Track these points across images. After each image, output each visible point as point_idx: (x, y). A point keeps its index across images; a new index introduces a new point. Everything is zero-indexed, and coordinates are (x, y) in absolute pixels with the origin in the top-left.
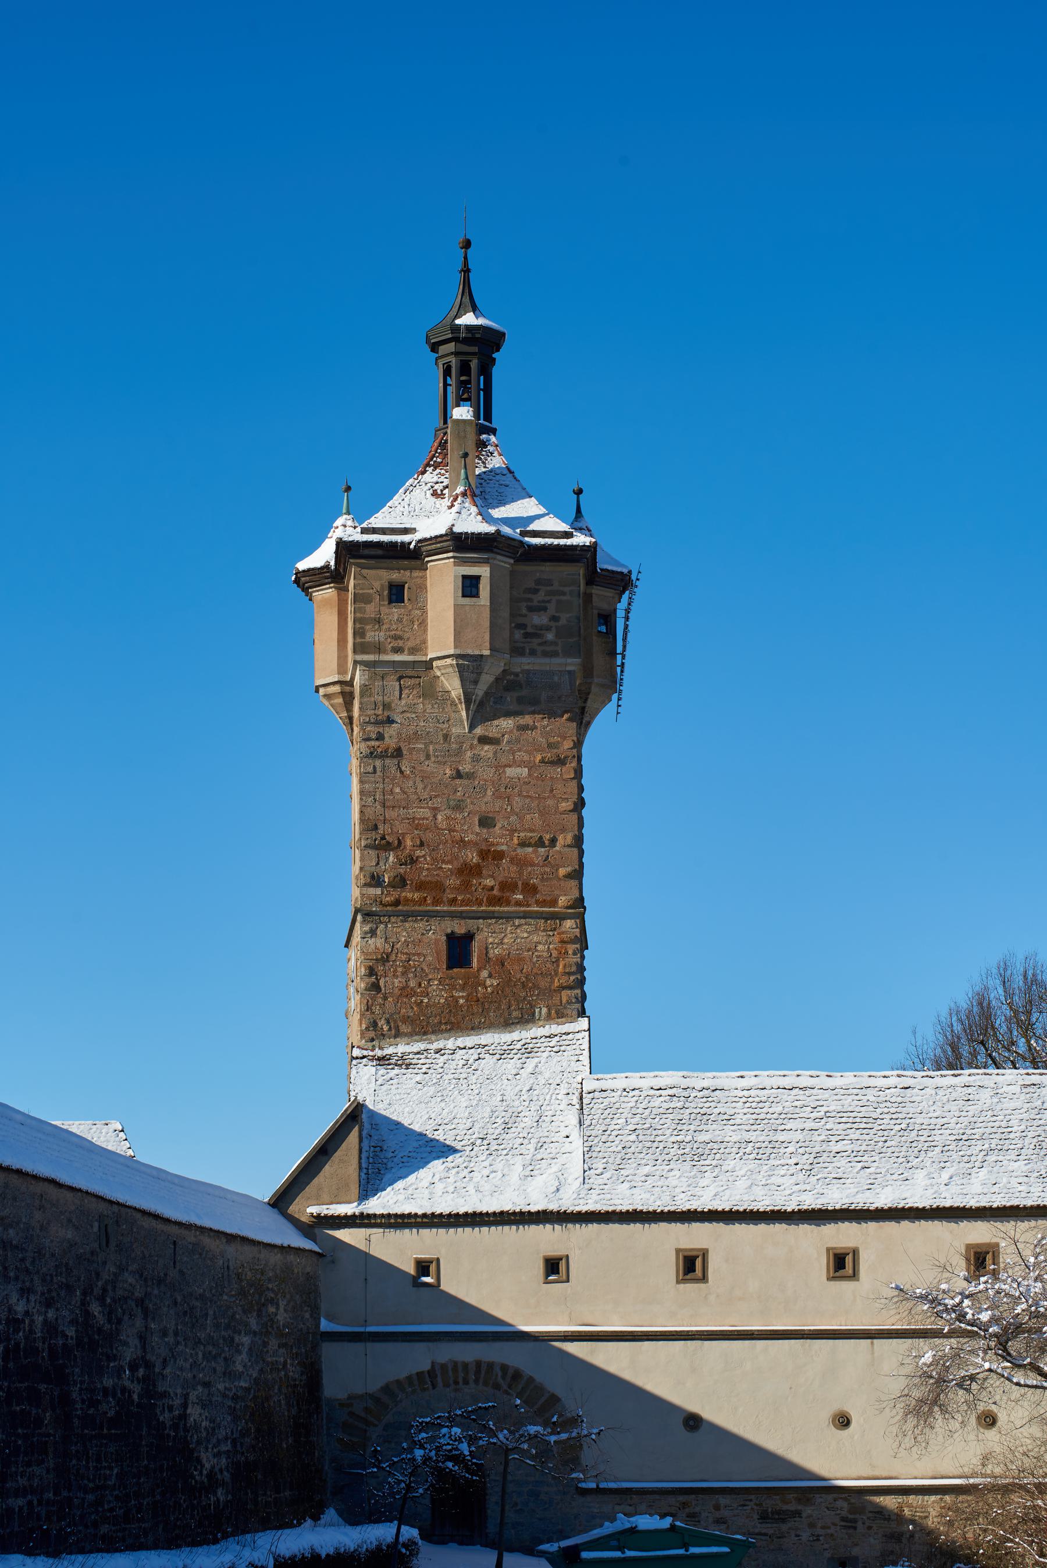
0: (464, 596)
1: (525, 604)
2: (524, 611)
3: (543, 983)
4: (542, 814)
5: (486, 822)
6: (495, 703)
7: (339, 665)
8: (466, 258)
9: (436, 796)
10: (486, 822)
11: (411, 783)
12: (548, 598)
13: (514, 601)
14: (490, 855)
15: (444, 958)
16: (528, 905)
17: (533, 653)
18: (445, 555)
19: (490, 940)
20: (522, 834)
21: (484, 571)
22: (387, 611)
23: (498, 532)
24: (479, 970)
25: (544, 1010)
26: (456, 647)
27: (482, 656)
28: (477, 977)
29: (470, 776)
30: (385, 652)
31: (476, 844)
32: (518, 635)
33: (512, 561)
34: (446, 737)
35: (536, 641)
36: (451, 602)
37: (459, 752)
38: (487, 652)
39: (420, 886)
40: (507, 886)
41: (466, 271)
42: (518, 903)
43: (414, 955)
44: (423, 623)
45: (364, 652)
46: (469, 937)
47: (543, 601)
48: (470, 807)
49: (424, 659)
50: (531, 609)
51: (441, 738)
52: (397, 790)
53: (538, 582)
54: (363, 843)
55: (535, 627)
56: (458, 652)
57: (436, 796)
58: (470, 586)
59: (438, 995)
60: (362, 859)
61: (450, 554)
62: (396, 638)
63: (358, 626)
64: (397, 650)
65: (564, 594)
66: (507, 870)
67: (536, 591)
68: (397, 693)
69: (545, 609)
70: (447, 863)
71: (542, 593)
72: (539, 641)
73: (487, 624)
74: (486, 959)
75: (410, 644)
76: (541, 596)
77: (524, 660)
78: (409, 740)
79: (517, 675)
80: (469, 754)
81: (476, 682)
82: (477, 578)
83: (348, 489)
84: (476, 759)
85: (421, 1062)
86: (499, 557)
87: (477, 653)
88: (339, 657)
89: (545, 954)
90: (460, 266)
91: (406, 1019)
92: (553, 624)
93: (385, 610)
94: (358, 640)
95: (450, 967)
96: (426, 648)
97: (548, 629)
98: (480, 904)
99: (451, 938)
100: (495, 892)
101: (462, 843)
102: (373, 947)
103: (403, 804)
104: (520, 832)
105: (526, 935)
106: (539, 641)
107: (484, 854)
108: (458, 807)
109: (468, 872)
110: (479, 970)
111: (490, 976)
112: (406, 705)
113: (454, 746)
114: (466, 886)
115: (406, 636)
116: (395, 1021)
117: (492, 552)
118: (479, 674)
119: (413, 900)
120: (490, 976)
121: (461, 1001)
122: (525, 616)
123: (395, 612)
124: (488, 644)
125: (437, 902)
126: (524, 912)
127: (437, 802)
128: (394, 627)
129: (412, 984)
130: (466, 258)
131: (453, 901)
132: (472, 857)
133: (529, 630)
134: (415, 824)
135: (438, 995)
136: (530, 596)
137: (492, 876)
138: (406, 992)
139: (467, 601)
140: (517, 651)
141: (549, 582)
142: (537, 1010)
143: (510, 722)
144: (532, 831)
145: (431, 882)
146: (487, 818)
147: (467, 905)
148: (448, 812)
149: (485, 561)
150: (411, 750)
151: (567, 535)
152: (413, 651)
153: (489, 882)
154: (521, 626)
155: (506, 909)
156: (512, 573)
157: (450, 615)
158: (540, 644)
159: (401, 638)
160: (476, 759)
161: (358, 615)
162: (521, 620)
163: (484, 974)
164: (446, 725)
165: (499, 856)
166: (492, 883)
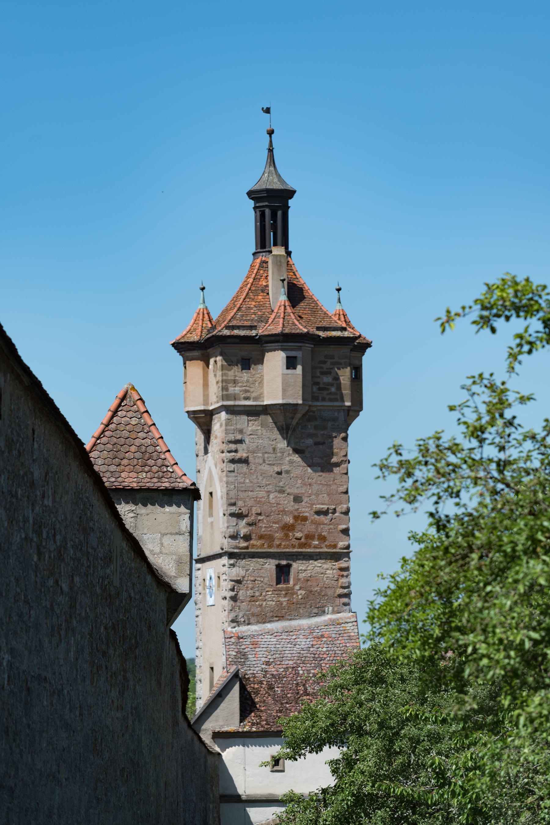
0: (288, 368)
1: (318, 370)
2: (318, 374)
3: (330, 592)
4: (328, 495)
5: (297, 499)
6: (302, 429)
7: (204, 400)
8: (271, 142)
9: (269, 484)
10: (297, 499)
11: (255, 477)
12: (332, 366)
13: (313, 368)
14: (300, 518)
15: (275, 579)
16: (321, 548)
17: (324, 399)
18: (276, 344)
19: (300, 568)
20: (318, 506)
21: (298, 354)
22: (241, 375)
23: (308, 333)
24: (294, 585)
25: (331, 608)
26: (283, 399)
27: (297, 404)
28: (292, 588)
29: (287, 472)
30: (239, 400)
31: (291, 512)
32: (315, 389)
33: (313, 346)
34: (274, 449)
35: (325, 392)
36: (281, 372)
37: (281, 458)
38: (300, 402)
39: (261, 537)
40: (309, 537)
41: (271, 150)
42: (315, 547)
43: (258, 577)
44: (261, 383)
45: (228, 400)
46: (289, 566)
47: (330, 368)
48: (289, 491)
49: (262, 403)
50: (322, 373)
51: (271, 450)
52: (247, 481)
53: (327, 357)
54: (229, 512)
55: (324, 384)
56: (284, 402)
57: (269, 484)
58: (291, 363)
59: (270, 601)
60: (228, 522)
61: (280, 344)
62: (246, 391)
63: (224, 384)
64: (247, 398)
65: (341, 364)
66: (309, 528)
67: (325, 362)
68: (246, 423)
69: (330, 373)
70: (275, 523)
71: (328, 363)
72: (328, 392)
73: (301, 385)
74: (297, 580)
75: (253, 395)
76: (328, 365)
77: (319, 404)
78: (253, 452)
79: (314, 412)
80: (287, 459)
81: (293, 418)
82: (295, 357)
83: (203, 289)
84: (291, 462)
85: (264, 640)
86: (307, 345)
87: (295, 402)
88: (204, 395)
89: (331, 576)
90: (267, 146)
91: (253, 615)
92: (335, 382)
93: (239, 374)
94: (225, 393)
95: (277, 584)
96: (263, 397)
97: (332, 385)
98: (294, 547)
99: (278, 566)
100: (303, 540)
101: (284, 512)
102: (235, 573)
103: (251, 489)
104: (316, 505)
105: (320, 565)
106: (328, 392)
107: (296, 518)
108: (282, 491)
109: (287, 528)
110: (294, 585)
111: (301, 588)
112: (252, 430)
113: (279, 455)
114: (287, 536)
115: (252, 390)
116: (248, 616)
117: (303, 342)
118: (295, 414)
119: (256, 546)
120: (301, 588)
121: (285, 603)
122: (319, 377)
123: (245, 376)
124: (301, 397)
125: (270, 546)
126: (319, 552)
127: (270, 488)
128: (245, 384)
129: (257, 594)
130: (271, 142)
131: (279, 546)
132: (290, 520)
133: (322, 386)
134: (258, 501)
135: (270, 601)
136: (322, 365)
137: (301, 531)
138: (253, 599)
139: (289, 371)
140: (315, 398)
141: (332, 357)
142: (326, 609)
143: (311, 440)
144: (323, 504)
145: (266, 535)
146: (298, 497)
147: (287, 548)
148: (276, 494)
149: (299, 349)
150: (255, 458)
151: (344, 329)
152: (256, 399)
153: (299, 535)
154: (317, 384)
155: (309, 550)
156: (312, 351)
157: (279, 381)
158: (328, 394)
159: (248, 391)
160: (291, 462)
161: (224, 378)
162: (317, 380)
163: (297, 587)
164: (274, 442)
165: (305, 519)
166: (300, 536)
